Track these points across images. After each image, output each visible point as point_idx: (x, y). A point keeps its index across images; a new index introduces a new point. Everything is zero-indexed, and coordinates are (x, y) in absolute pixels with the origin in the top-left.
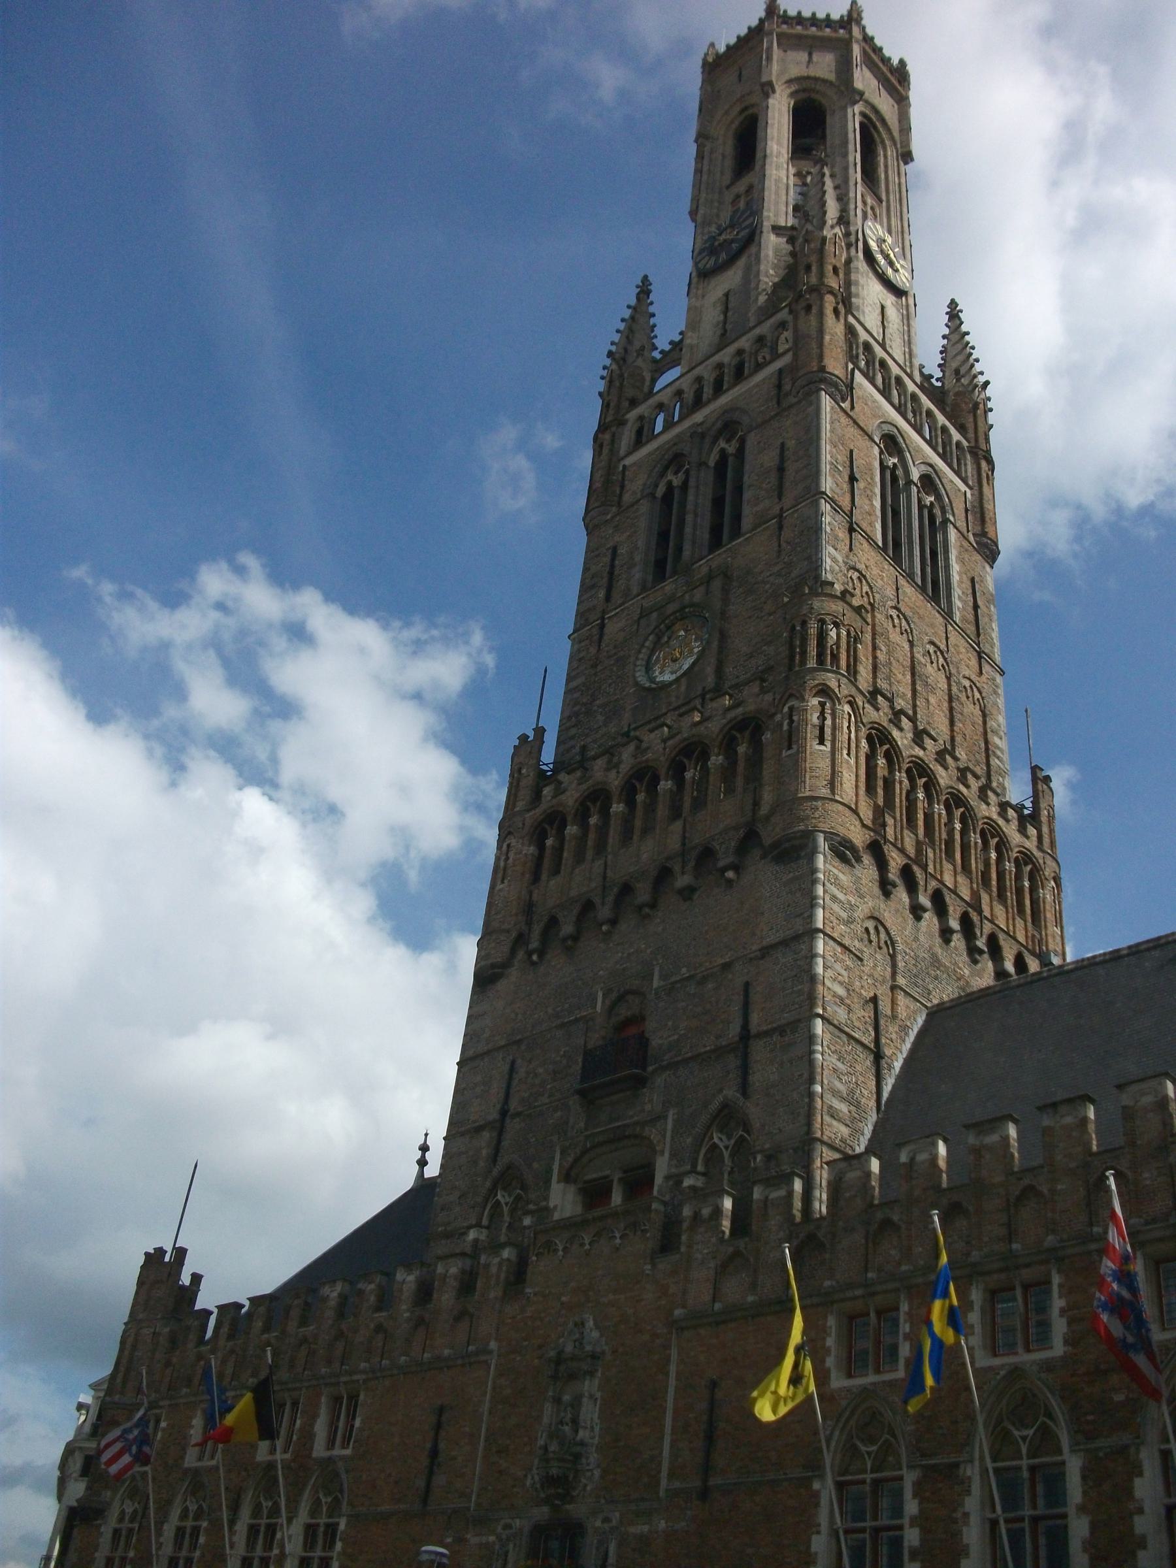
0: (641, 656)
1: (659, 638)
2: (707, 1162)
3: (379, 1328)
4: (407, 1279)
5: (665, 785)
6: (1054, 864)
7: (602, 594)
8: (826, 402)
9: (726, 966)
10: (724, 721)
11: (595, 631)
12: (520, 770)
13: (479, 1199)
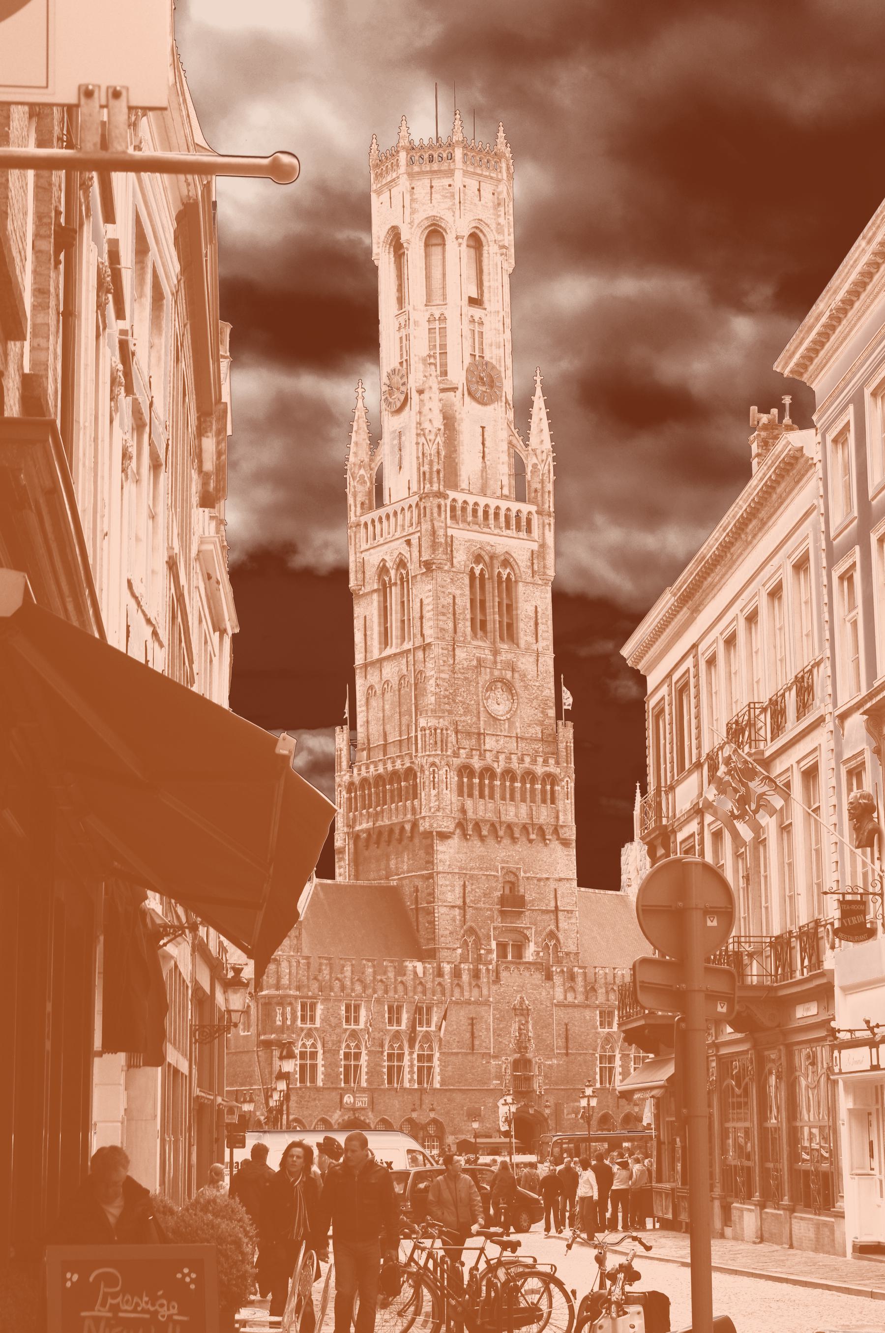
5: (518, 785)
9: (548, 879)
10: (543, 770)
11: (450, 648)
12: (447, 730)
13: (459, 937)
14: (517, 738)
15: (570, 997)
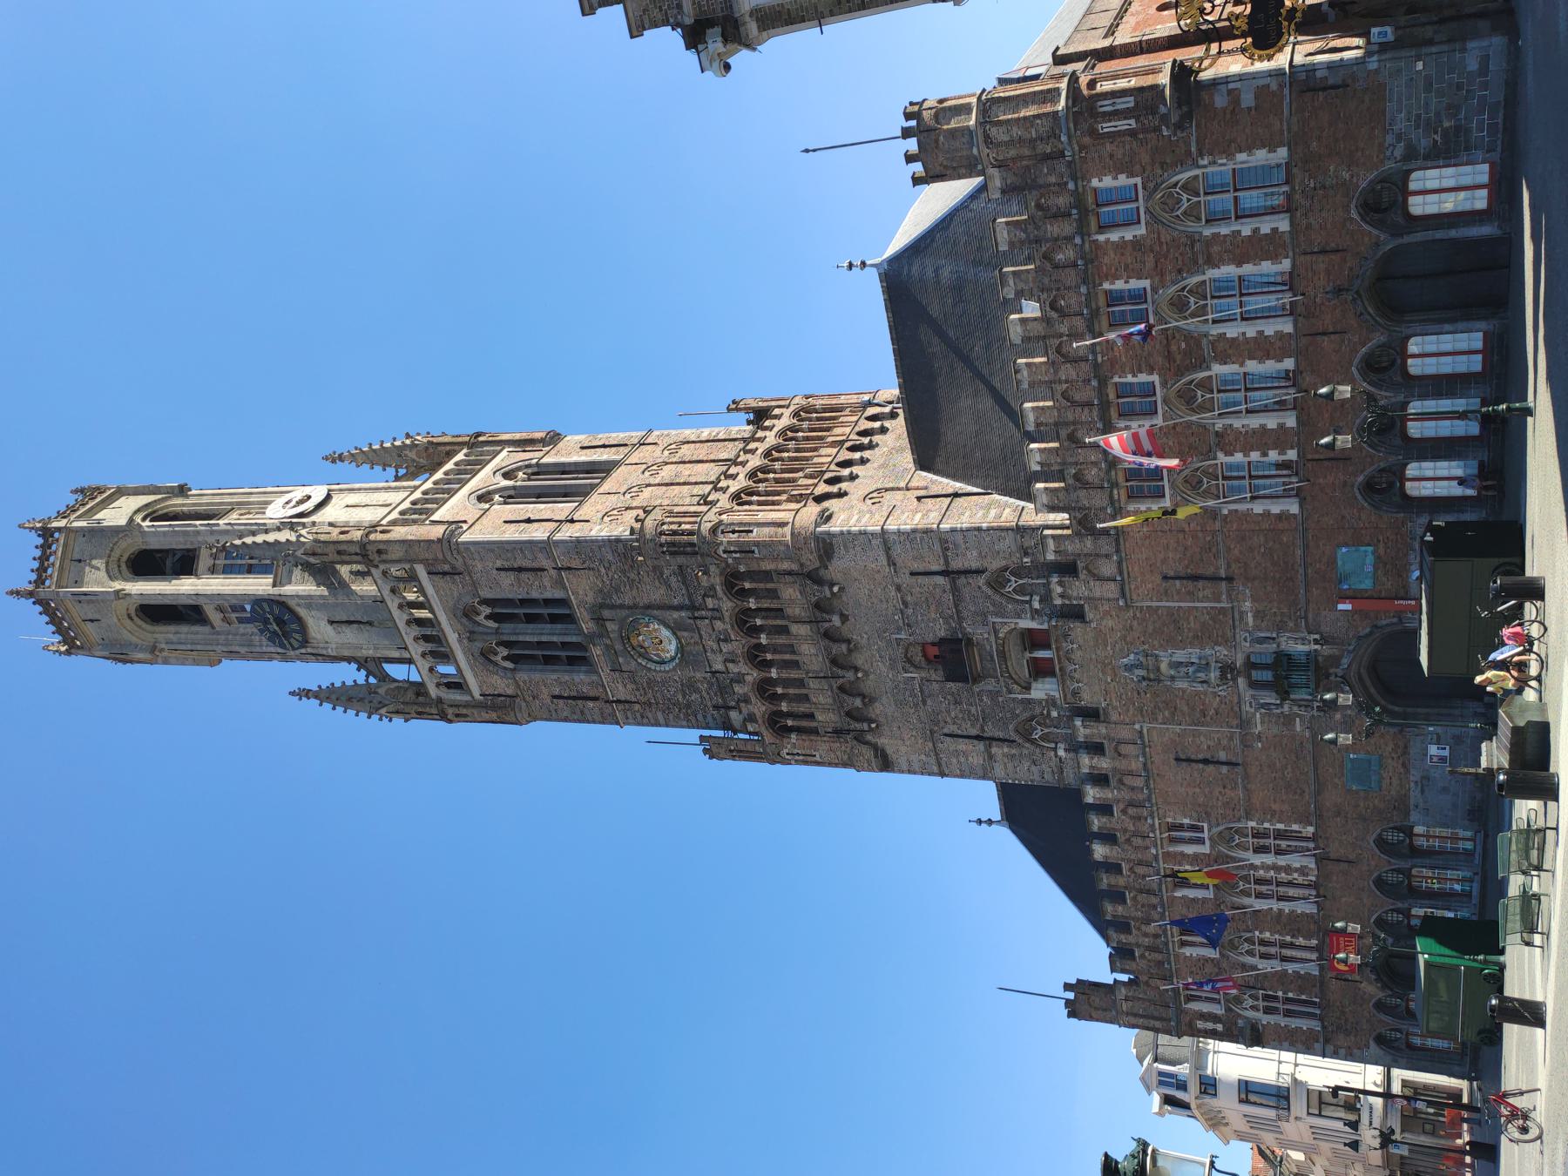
0: (653, 668)
1: (640, 655)
2: (1025, 595)
3: (1124, 812)
4: (1091, 794)
5: (764, 639)
6: (797, 398)
7: (591, 704)
8: (464, 538)
9: (898, 588)
11: (621, 707)
12: (731, 751)
13: (1038, 750)
14: (696, 618)
15: (1107, 568)
